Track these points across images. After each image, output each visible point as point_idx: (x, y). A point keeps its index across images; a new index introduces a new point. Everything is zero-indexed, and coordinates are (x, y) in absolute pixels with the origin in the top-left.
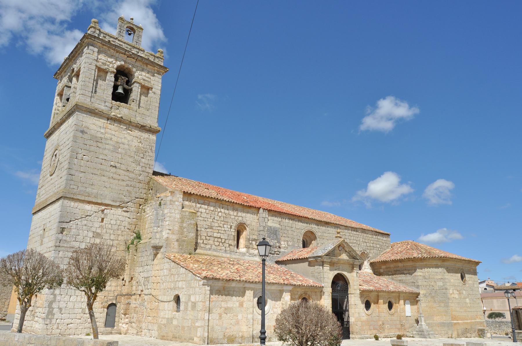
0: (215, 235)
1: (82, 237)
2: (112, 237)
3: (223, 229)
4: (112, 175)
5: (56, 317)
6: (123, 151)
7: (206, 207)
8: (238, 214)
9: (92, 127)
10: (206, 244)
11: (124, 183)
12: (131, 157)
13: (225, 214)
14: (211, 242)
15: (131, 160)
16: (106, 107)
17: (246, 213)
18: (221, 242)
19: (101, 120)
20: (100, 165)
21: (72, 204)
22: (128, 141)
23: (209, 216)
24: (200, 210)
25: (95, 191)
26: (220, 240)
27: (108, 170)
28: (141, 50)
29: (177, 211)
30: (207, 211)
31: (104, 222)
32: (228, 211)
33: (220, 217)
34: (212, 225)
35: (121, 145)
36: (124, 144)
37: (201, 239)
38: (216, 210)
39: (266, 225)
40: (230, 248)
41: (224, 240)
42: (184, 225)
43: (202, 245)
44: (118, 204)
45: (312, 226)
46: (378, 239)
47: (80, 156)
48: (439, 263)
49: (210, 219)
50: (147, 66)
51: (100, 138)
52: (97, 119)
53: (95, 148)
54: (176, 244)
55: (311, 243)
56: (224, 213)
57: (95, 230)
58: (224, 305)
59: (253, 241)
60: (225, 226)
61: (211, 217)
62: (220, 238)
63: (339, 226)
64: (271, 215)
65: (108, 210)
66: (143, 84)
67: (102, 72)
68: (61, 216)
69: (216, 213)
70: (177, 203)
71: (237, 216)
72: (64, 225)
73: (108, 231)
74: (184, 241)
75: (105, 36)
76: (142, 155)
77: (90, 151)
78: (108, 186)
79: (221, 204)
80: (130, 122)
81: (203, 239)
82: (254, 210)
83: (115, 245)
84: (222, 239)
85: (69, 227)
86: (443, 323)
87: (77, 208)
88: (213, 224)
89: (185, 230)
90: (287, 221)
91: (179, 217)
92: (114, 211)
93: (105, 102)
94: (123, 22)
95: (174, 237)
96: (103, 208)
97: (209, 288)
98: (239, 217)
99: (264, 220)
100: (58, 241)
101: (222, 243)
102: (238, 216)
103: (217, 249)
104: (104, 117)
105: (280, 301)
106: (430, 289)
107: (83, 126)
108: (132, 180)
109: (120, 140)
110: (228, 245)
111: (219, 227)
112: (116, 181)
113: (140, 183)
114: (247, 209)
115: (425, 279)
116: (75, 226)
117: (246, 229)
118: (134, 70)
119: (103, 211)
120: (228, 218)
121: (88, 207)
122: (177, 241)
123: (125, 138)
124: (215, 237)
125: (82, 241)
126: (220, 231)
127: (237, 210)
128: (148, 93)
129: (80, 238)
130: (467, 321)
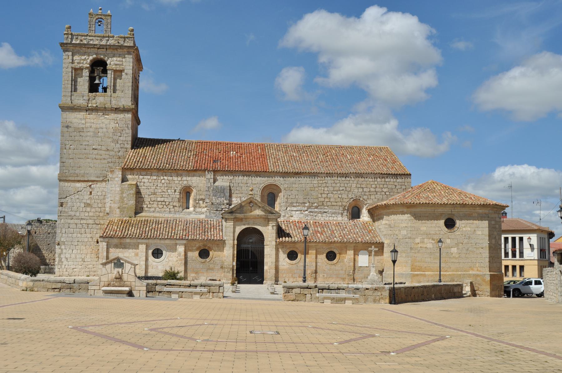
0: (159, 199)
1: (76, 208)
2: (100, 205)
3: (167, 194)
4: (94, 156)
5: (64, 263)
6: (102, 135)
7: (149, 177)
8: (183, 178)
9: (75, 121)
10: (150, 208)
11: (106, 161)
12: (109, 138)
13: (169, 181)
14: (155, 206)
15: (110, 140)
16: (84, 101)
17: (192, 176)
18: (165, 205)
19: (81, 113)
20: (84, 151)
21: (66, 184)
22: (106, 125)
23: (152, 184)
24: (143, 180)
25: (82, 172)
26: (164, 203)
27: (91, 153)
28: (111, 37)
29: (117, 186)
31: (92, 194)
32: (171, 178)
33: (163, 184)
34: (155, 192)
35: (100, 130)
38: (159, 178)
39: (211, 185)
42: (124, 195)
43: (146, 209)
44: (101, 179)
45: (276, 179)
46: (386, 182)
47: (68, 146)
48: (405, 210)
51: (81, 129)
52: (78, 113)
54: (118, 210)
55: (278, 196)
56: (167, 180)
57: (85, 202)
59: (200, 200)
60: (169, 191)
61: (154, 185)
62: (164, 201)
63: (317, 174)
64: (221, 174)
65: (94, 185)
66: (115, 69)
67: (77, 71)
68: (60, 194)
69: (159, 181)
70: (116, 179)
71: (181, 181)
72: (62, 201)
73: (96, 201)
74: (125, 208)
75: (77, 37)
76: (119, 134)
77: (75, 141)
78: (92, 166)
79: (164, 172)
80: (105, 108)
82: (200, 172)
83: (103, 211)
84: (165, 202)
85: (66, 201)
86: (402, 274)
87: (70, 187)
89: (125, 199)
90: (241, 178)
91: (119, 190)
92: (99, 185)
93: (83, 96)
94: (91, 16)
95: (117, 206)
96: (90, 183)
97: (106, 244)
98: (184, 181)
99: (209, 181)
100: (60, 212)
101: (166, 206)
102: (183, 180)
103: (161, 211)
104: (84, 110)
105: (176, 251)
106: (394, 238)
108: (112, 157)
109: (98, 126)
112: (99, 161)
113: (119, 158)
114: (193, 173)
115: (391, 227)
116: (70, 200)
117: (192, 191)
118: (106, 59)
119: (90, 186)
121: (78, 185)
122: (119, 208)
123: (103, 123)
124: (159, 201)
125: (76, 210)
126: (164, 196)
127: (181, 175)
128: (121, 75)
129: (75, 208)
130: (445, 273)
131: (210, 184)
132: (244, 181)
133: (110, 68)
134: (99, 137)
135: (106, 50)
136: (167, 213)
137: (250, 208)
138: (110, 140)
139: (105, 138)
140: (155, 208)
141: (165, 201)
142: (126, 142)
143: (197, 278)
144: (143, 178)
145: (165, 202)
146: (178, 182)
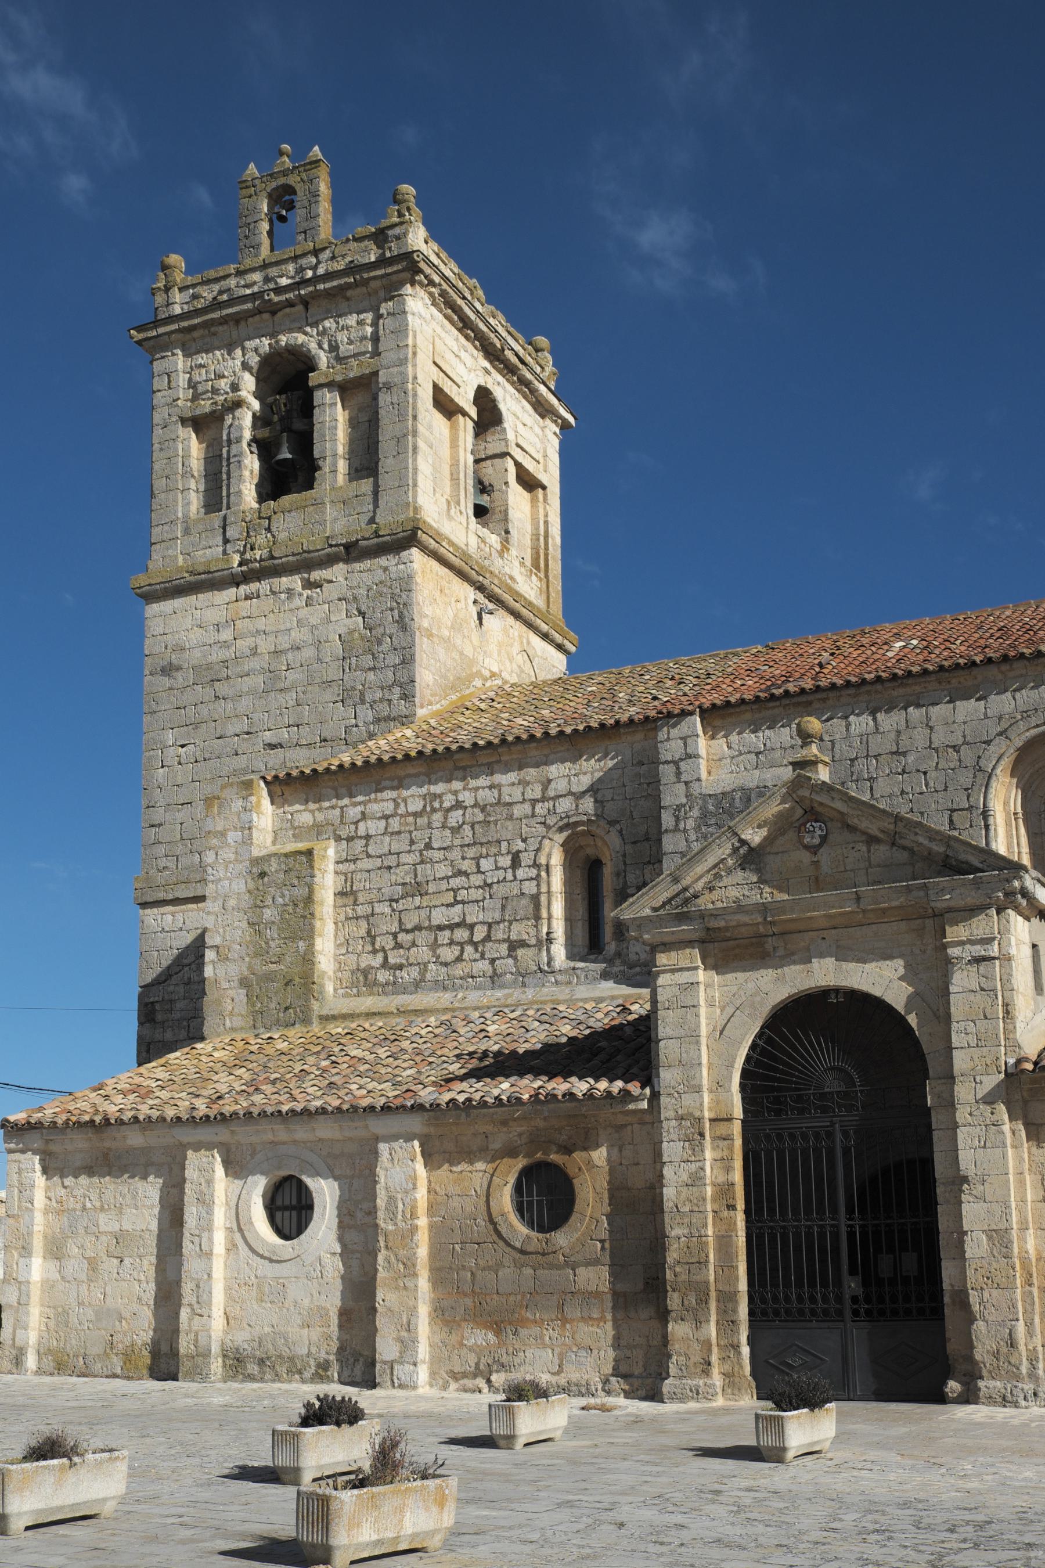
0: (439, 917)
3: (476, 880)
10: (400, 967)
13: (483, 809)
14: (423, 953)
15: (329, 695)
18: (471, 942)
23: (400, 844)
26: (461, 934)
30: (395, 824)
33: (456, 830)
34: (419, 879)
36: (298, 648)
37: (374, 952)
38: (437, 805)
40: (515, 959)
41: (485, 928)
42: (268, 913)
49: (409, 852)
50: (348, 299)
53: (211, 706)
58: (107, 1223)
61: (412, 842)
71: (543, 799)
77: (196, 725)
79: (457, 768)
81: (383, 949)
84: (471, 927)
88: (425, 871)
90: (861, 723)
99: (678, 774)
101: (475, 945)
102: (551, 793)
109: (284, 642)
110: (505, 946)
111: (454, 876)
120: (496, 822)
124: (440, 928)
126: (462, 895)
131: (682, 786)
132: (882, 744)
134: (289, 689)
135: (307, 309)
136: (478, 988)
137: (806, 857)
138: (329, 695)
139: (310, 688)
140: (424, 966)
141: (470, 920)
142: (397, 690)
143: (504, 1359)
144: (364, 816)
145: (471, 927)
146: (527, 808)
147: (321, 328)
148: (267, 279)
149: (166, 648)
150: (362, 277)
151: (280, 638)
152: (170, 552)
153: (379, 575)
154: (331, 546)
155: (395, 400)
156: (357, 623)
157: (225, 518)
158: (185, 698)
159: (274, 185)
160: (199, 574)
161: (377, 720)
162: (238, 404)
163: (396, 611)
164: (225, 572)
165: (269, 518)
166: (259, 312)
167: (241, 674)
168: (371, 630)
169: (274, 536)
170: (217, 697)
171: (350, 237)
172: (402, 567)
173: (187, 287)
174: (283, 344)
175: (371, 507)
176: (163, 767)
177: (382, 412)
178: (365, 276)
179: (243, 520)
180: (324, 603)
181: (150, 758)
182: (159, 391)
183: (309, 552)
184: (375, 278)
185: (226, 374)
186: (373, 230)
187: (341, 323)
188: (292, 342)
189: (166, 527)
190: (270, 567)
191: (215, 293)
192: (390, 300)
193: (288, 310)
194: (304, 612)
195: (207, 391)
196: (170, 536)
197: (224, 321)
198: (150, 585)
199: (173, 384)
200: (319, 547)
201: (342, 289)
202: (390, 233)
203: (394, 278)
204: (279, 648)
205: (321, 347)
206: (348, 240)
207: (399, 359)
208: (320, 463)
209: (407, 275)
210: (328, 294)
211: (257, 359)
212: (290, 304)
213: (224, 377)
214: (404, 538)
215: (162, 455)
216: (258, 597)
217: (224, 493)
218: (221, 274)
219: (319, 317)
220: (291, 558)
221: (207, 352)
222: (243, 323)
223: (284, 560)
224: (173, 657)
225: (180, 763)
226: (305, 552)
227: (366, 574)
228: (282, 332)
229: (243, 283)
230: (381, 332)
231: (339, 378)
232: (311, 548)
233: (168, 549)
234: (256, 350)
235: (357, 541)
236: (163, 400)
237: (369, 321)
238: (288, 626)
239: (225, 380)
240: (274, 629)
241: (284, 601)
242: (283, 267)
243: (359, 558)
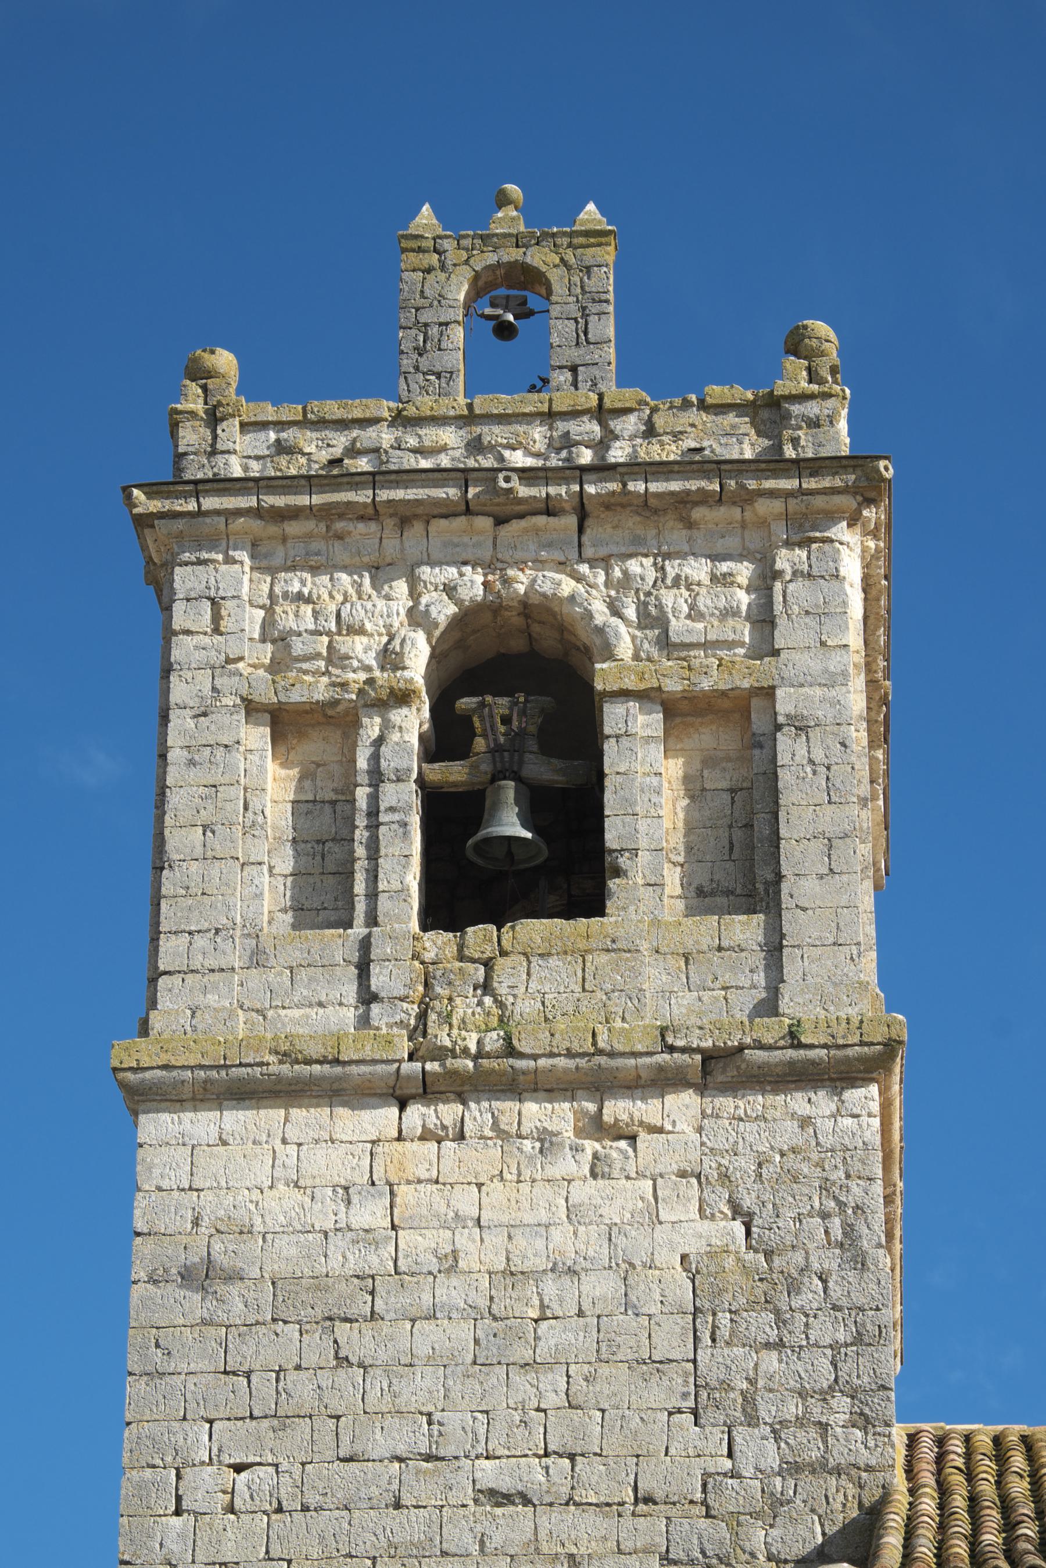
20: (393, 1519)
36: (571, 1272)
53: (325, 1379)
77: (281, 1420)
107: (205, 1222)
133: (630, 683)
134: (549, 1366)
139: (604, 1370)
147: (617, 573)
148: (476, 446)
149: (196, 1222)
150: (743, 487)
151: (520, 1241)
152: (212, 999)
153: (789, 1133)
154: (672, 1049)
155: (818, 755)
156: (731, 1234)
157: (365, 945)
158: (249, 1350)
159: (491, 258)
160: (308, 1062)
161: (792, 1468)
162: (403, 697)
163: (837, 1221)
164: (380, 1068)
165: (488, 964)
166: (468, 510)
167: (414, 1312)
168: (769, 1255)
169: (500, 1004)
170: (342, 1361)
171: (693, 398)
172: (848, 1122)
173: (264, 425)
174: (521, 589)
175: (760, 978)
176: (178, 1512)
177: (785, 777)
178: (752, 484)
179: (416, 956)
180: (640, 1175)
181: (141, 1485)
182: (188, 632)
183: (612, 1055)
184: (772, 494)
185: (369, 626)
186: (750, 396)
187: (671, 571)
188: (547, 588)
189: (200, 941)
190: (502, 1073)
191: (337, 452)
192: (800, 545)
193: (541, 520)
194: (585, 1191)
195: (318, 656)
196: (211, 962)
197: (373, 513)
198: (165, 1067)
199: (225, 625)
200: (639, 1048)
201: (683, 501)
202: (796, 409)
203: (819, 502)
204: (517, 1265)
205: (616, 612)
206: (686, 405)
207: (826, 671)
208: (623, 861)
209: (848, 502)
210: (646, 505)
211: (452, 609)
212: (549, 508)
213: (361, 631)
214: (861, 1059)
215: (193, 773)
216: (461, 1137)
217: (360, 887)
218: (357, 414)
219: (615, 550)
220: (562, 1062)
221: (315, 570)
222: (418, 527)
223: (542, 1062)
224: (217, 1247)
225: (231, 1509)
226: (600, 1052)
227: (754, 1126)
228: (521, 565)
229: (412, 442)
230: (778, 607)
231: (673, 686)
232: (619, 1047)
233: (205, 991)
234: (450, 590)
235: (741, 1049)
236: (200, 656)
237: (743, 579)
238: (543, 1216)
239: (365, 639)
240: (505, 1219)
241: (531, 1158)
242: (520, 429)
243: (733, 1088)
